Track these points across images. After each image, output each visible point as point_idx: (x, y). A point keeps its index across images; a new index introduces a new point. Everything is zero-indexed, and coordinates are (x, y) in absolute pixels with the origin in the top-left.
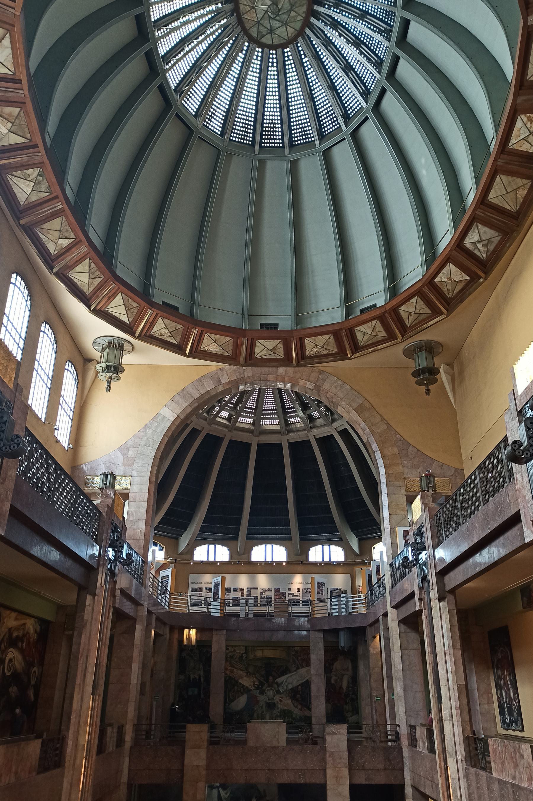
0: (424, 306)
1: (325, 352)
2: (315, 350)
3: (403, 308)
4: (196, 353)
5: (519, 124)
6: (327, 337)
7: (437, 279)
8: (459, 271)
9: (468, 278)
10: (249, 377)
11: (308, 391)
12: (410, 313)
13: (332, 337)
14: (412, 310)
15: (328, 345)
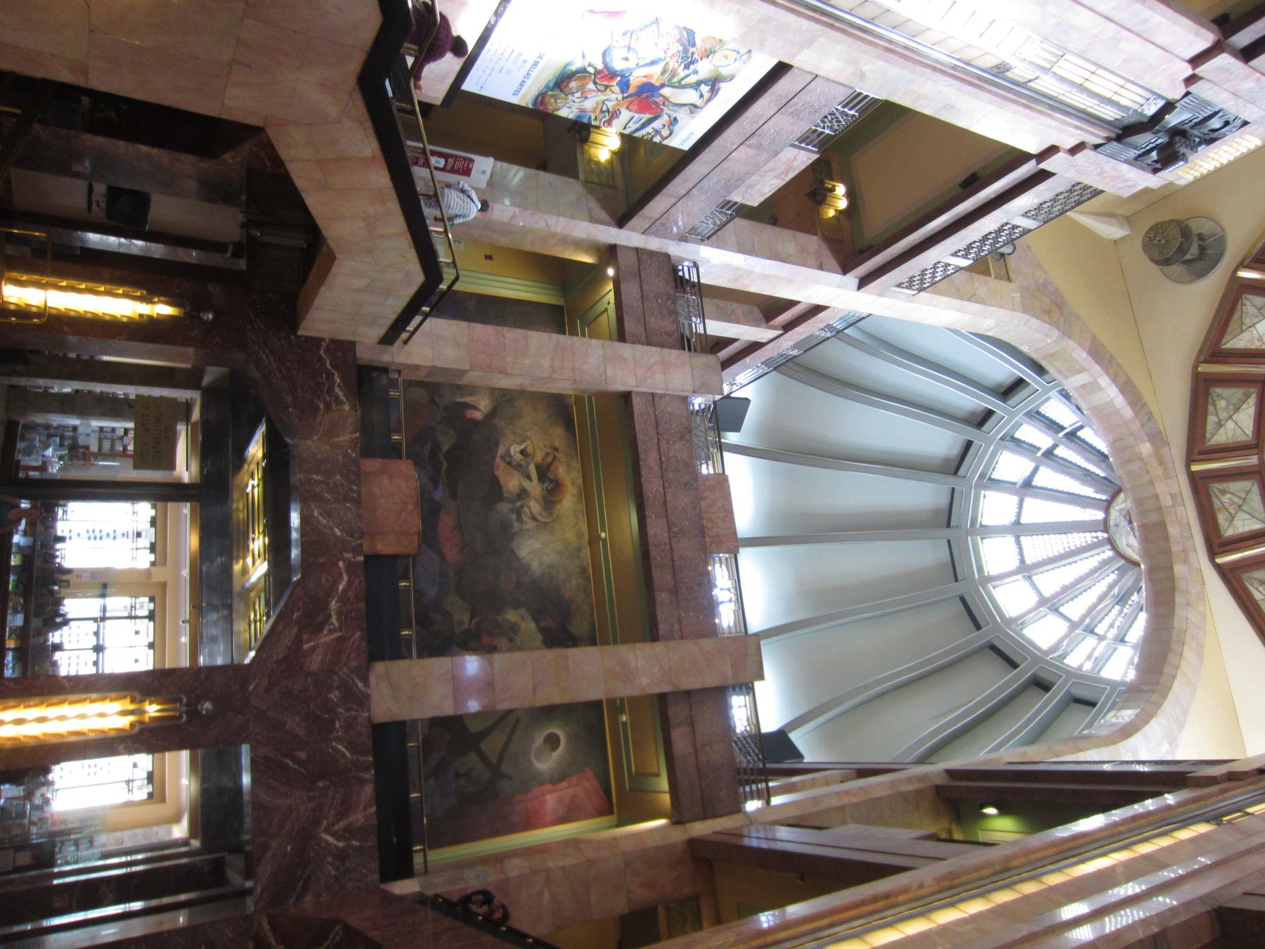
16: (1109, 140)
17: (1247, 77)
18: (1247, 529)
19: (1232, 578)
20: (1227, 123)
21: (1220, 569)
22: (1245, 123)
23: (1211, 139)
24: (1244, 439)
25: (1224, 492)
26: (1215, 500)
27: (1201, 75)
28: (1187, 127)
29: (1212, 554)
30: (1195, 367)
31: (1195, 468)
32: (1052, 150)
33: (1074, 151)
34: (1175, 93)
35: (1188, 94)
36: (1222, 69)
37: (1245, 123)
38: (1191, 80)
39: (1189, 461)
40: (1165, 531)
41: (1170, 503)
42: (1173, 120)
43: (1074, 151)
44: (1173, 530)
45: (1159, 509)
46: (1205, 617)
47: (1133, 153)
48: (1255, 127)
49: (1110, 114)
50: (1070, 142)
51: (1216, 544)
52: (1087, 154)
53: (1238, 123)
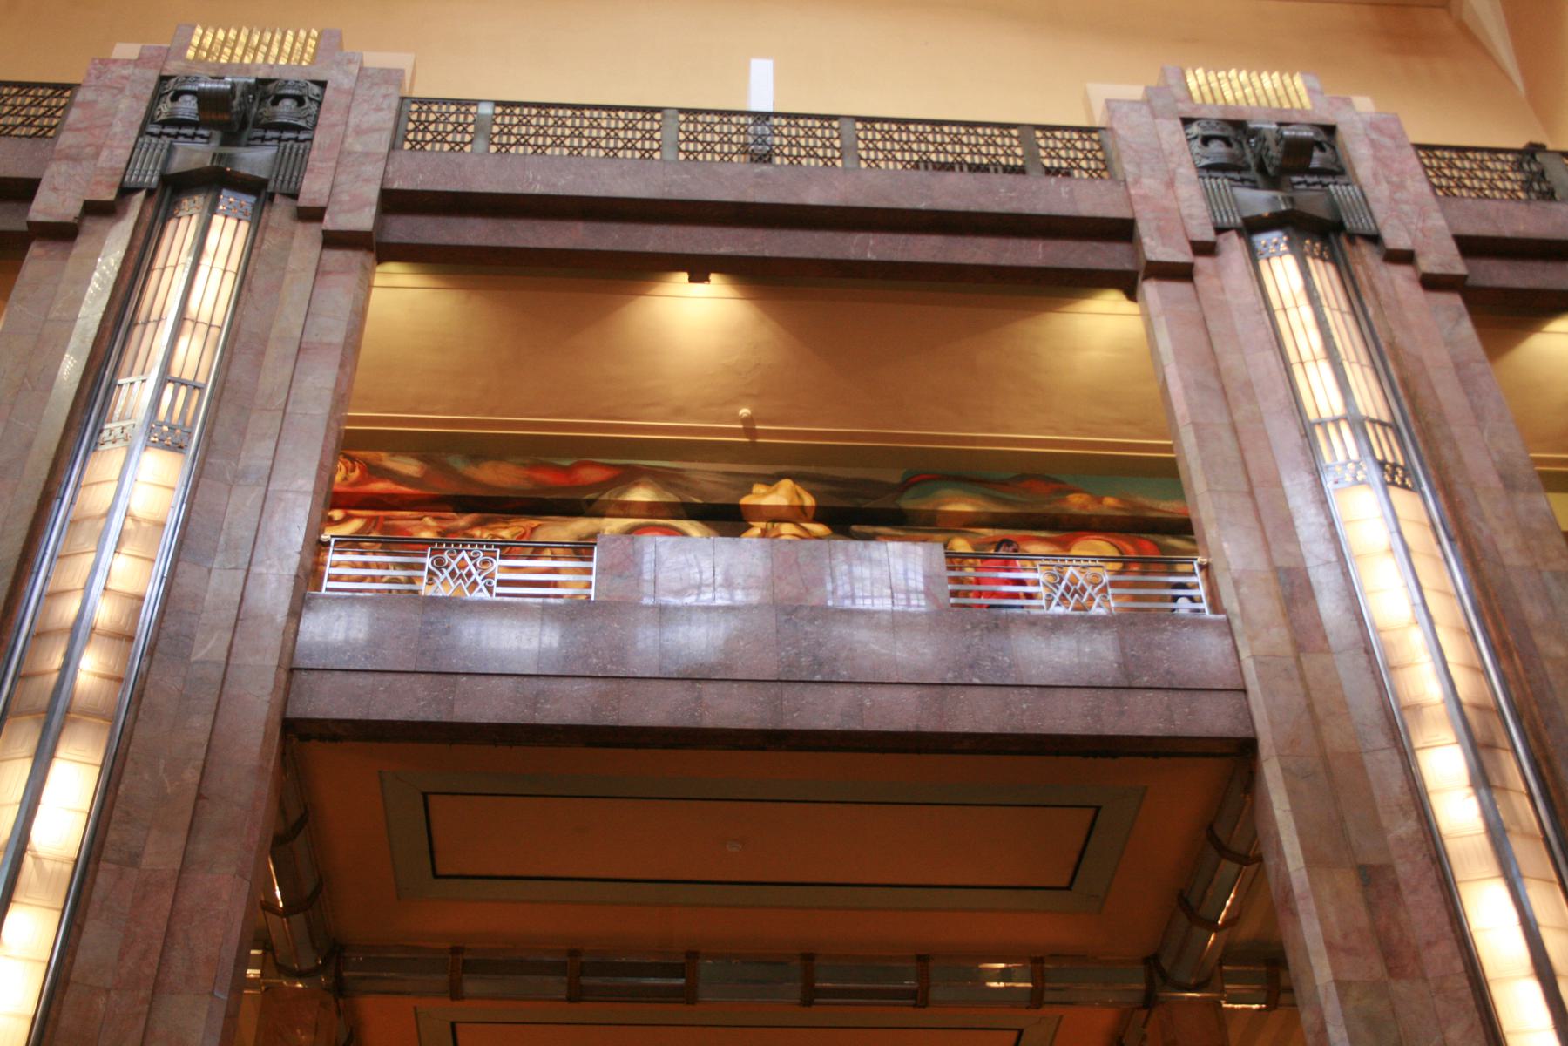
16: (1352, 238)
17: (1145, 197)
20: (1206, 140)
22: (1187, 122)
23: (1236, 129)
27: (1188, 248)
28: (1253, 174)
32: (1431, 283)
33: (1404, 258)
34: (1233, 246)
35: (1219, 230)
36: (1162, 233)
37: (1187, 122)
38: (1204, 249)
42: (1259, 201)
43: (1404, 258)
47: (1337, 190)
48: (1181, 106)
49: (1324, 276)
50: (1400, 277)
52: (1397, 239)
53: (1195, 129)
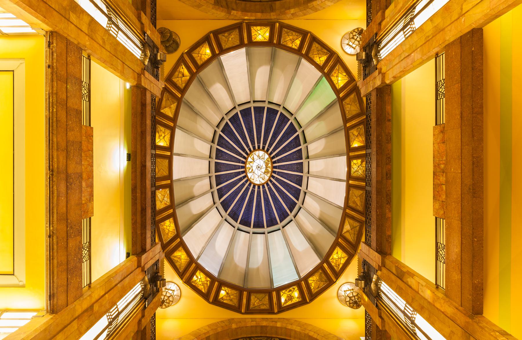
0: (177, 83)
1: (226, 34)
2: (233, 36)
3: (188, 78)
4: (304, 34)
5: (169, 201)
6: (227, 47)
7: (176, 104)
8: (167, 114)
9: (162, 111)
10: (273, 16)
11: (235, 7)
12: (183, 76)
13: (223, 47)
14: (183, 78)
15: (225, 41)
18: (267, 301)
19: (282, 309)
21: (279, 312)
24: (238, 294)
25: (254, 304)
26: (256, 308)
29: (273, 313)
30: (209, 302)
31: (243, 311)
39: (240, 312)
40: (264, 326)
41: (255, 323)
44: (264, 324)
45: (256, 326)
46: (296, 321)
51: (270, 311)
